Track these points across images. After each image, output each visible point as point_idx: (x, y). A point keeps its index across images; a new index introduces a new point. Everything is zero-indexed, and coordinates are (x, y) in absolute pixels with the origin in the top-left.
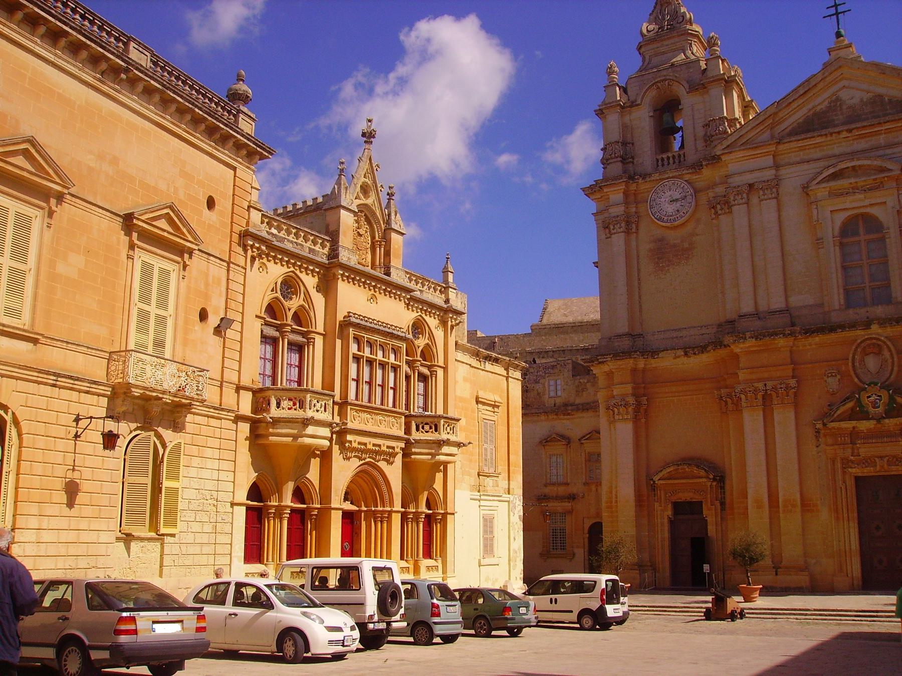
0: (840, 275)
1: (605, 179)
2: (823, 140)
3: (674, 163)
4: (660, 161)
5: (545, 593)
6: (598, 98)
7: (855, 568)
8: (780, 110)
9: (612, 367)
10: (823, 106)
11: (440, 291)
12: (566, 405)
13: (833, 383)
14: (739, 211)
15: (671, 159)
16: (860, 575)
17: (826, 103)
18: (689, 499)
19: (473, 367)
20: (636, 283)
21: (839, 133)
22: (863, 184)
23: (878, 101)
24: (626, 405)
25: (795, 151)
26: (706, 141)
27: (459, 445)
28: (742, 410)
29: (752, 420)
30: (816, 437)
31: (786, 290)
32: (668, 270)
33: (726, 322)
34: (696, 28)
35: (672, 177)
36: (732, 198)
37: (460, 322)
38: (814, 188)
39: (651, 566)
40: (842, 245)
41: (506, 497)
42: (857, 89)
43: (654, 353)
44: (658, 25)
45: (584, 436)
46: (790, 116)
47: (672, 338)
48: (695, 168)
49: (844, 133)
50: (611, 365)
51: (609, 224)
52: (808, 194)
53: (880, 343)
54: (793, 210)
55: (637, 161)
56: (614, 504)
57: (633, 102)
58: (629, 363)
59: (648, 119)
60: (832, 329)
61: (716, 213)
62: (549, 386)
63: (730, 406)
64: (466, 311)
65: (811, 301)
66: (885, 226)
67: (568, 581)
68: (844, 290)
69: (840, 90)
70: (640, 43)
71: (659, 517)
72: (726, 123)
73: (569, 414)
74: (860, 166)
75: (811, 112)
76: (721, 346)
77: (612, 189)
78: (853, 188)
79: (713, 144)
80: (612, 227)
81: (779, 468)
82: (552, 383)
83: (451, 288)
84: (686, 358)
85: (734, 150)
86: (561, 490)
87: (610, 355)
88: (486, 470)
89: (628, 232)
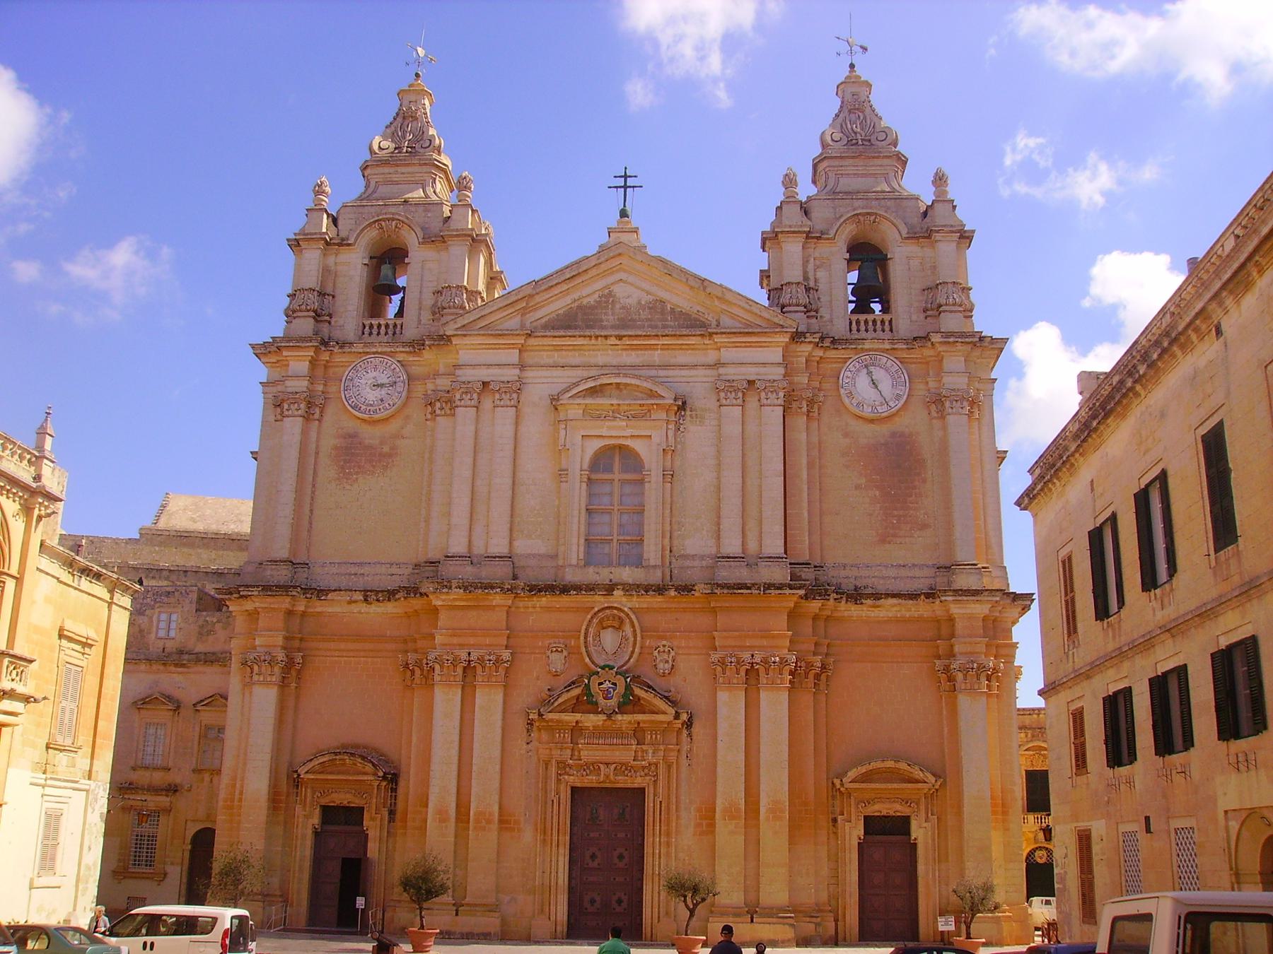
0: (583, 521)
1: (287, 338)
2: (585, 343)
3: (386, 333)
4: (367, 328)
5: (136, 933)
6: (296, 223)
7: (561, 910)
8: (537, 294)
9: (257, 605)
10: (591, 300)
11: (29, 461)
12: (181, 652)
13: (557, 661)
14: (465, 415)
15: (383, 328)
16: (566, 918)
17: (596, 296)
19: (61, 582)
20: (309, 491)
21: (606, 337)
22: (626, 408)
23: (658, 306)
24: (272, 662)
25: (548, 350)
26: (434, 313)
27: (27, 699)
28: (433, 684)
29: (446, 701)
31: (511, 530)
32: (357, 479)
33: (426, 562)
34: (445, 159)
36: (458, 396)
37: (54, 513)
38: (565, 402)
39: (281, 896)
40: (590, 481)
41: (85, 783)
42: (638, 288)
43: (321, 593)
44: (396, 143)
45: (202, 701)
46: (548, 304)
47: (350, 574)
48: (414, 347)
49: (613, 338)
50: (256, 602)
51: (283, 401)
52: (556, 409)
54: (535, 426)
55: (336, 322)
56: (236, 803)
57: (343, 240)
58: (284, 603)
59: (360, 266)
60: (565, 590)
62: (159, 621)
64: (63, 496)
65: (543, 550)
66: (647, 467)
67: (172, 916)
68: (586, 540)
70: (366, 161)
71: (300, 825)
72: (465, 295)
73: (183, 666)
74: (626, 385)
75: (576, 304)
79: (443, 320)
80: (286, 406)
81: (474, 768)
82: (164, 617)
83: (47, 459)
84: (365, 604)
85: (469, 333)
86: (158, 778)
87: (258, 586)
88: (60, 740)
89: (307, 417)
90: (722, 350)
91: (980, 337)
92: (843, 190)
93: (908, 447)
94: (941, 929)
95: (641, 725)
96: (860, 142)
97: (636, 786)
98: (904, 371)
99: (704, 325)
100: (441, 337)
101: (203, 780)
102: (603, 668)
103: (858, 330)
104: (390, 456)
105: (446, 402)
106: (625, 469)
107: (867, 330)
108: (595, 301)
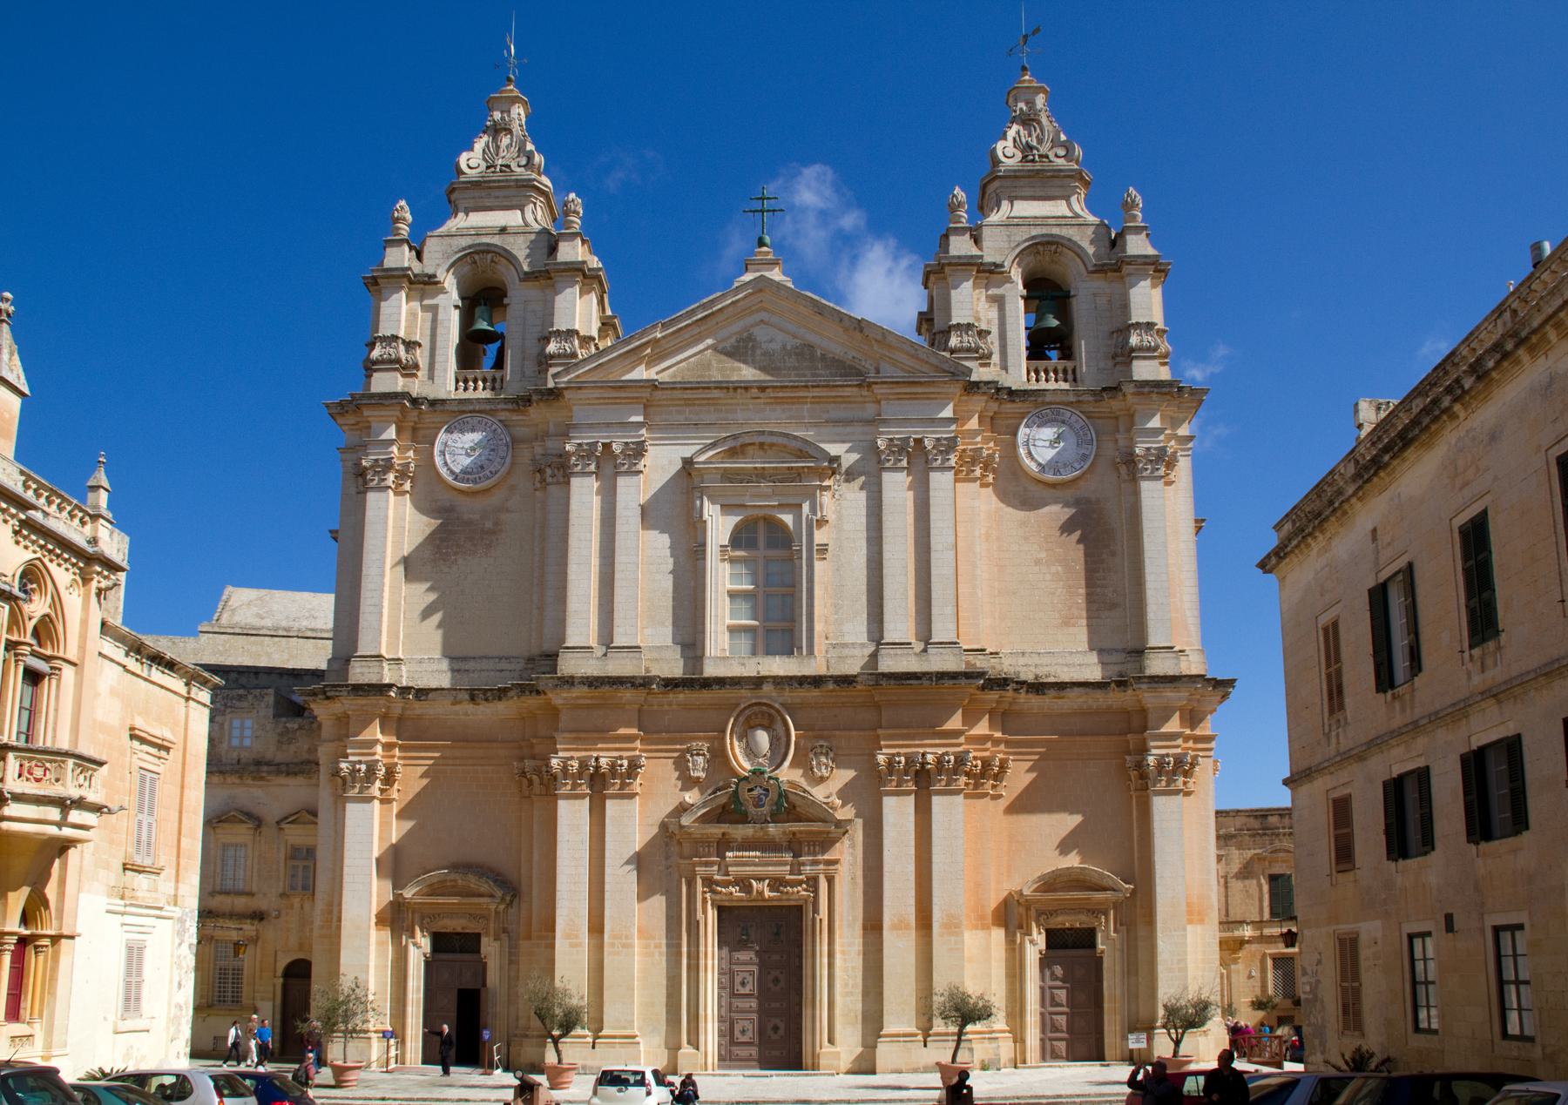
2: (722, 395)
17: (733, 340)
18: (459, 930)
30: (667, 845)
33: (541, 656)
35: (479, 412)
42: (780, 330)
44: (487, 161)
48: (518, 404)
52: (690, 474)
53: (773, 711)
61: (543, 480)
63: (537, 787)
69: (757, 324)
76: (531, 692)
77: (376, 413)
78: (757, 476)
84: (471, 706)
90: (882, 402)
91: (1179, 388)
92: (1018, 215)
93: (1095, 516)
94: (1131, 1046)
95: (798, 836)
96: (1037, 157)
97: (793, 903)
98: (1091, 428)
99: (859, 373)
100: (551, 392)
101: (292, 907)
102: (754, 772)
103: (1037, 380)
104: (493, 532)
105: (558, 469)
106: (771, 544)
107: (1047, 380)
108: (733, 346)
